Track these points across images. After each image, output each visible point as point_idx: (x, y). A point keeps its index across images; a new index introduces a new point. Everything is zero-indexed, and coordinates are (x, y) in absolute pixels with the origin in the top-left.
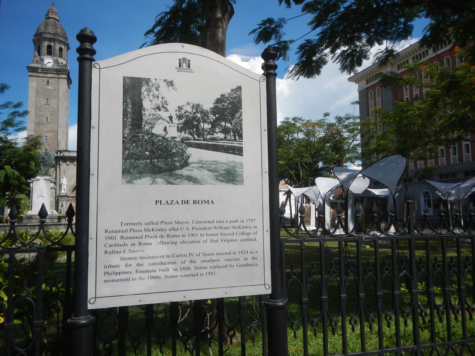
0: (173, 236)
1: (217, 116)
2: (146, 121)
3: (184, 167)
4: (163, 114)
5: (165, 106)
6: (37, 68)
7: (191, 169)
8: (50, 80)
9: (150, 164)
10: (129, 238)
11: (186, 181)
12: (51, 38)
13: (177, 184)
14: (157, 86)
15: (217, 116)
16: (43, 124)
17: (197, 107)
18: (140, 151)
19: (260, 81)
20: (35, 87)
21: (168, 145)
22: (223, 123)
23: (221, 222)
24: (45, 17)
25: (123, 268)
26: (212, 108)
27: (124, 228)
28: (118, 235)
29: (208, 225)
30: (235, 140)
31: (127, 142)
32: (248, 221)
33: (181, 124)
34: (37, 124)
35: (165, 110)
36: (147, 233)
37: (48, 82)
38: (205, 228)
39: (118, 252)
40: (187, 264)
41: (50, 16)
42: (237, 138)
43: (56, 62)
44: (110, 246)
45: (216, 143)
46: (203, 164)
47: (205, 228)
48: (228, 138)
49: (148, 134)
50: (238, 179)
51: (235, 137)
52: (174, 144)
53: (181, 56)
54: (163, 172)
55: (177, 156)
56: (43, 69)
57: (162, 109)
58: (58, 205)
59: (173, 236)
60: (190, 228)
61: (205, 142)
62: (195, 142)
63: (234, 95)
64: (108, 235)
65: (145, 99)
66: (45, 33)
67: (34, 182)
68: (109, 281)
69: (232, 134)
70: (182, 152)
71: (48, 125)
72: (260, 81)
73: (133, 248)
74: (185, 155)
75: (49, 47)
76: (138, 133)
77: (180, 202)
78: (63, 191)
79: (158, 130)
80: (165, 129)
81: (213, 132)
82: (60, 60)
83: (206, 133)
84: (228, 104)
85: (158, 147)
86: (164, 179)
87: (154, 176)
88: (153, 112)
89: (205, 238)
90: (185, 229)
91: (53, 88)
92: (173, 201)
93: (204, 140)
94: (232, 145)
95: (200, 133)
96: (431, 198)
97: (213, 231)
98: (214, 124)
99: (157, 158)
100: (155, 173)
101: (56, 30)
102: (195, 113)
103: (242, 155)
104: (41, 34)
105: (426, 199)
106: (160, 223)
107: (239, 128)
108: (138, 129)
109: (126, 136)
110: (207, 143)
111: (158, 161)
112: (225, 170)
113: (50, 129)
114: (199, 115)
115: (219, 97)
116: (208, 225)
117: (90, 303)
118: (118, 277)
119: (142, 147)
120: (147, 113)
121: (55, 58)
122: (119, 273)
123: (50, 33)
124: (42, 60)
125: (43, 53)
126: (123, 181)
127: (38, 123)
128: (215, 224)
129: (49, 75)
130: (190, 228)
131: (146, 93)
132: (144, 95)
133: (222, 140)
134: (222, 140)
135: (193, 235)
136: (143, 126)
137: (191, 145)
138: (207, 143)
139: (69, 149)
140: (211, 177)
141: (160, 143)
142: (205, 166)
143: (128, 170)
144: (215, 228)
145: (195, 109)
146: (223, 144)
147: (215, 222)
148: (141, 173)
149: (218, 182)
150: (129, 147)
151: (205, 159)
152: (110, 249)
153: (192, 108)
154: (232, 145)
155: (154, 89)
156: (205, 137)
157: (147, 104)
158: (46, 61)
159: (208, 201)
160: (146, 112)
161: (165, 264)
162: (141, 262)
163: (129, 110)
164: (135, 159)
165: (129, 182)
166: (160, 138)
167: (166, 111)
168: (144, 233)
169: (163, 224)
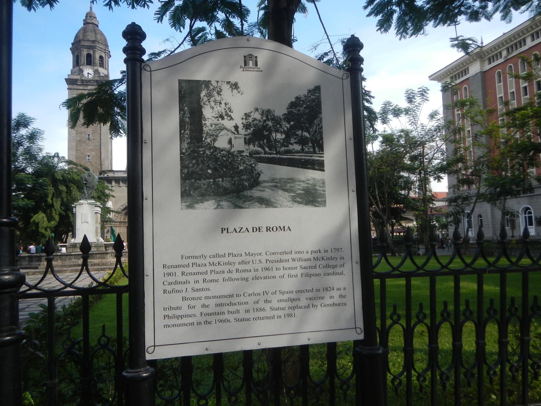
0: (243, 271)
1: (292, 123)
2: (207, 133)
3: (254, 187)
4: (227, 123)
5: (230, 113)
6: (76, 80)
7: (262, 189)
9: (213, 184)
10: (191, 274)
11: (256, 204)
12: (90, 46)
13: (246, 208)
14: (219, 90)
15: (292, 123)
16: (84, 142)
17: (267, 113)
18: (202, 170)
19: (342, 79)
21: (234, 160)
22: (299, 132)
23: (300, 252)
24: (82, 22)
25: (185, 311)
26: (285, 114)
27: (185, 262)
28: (179, 271)
29: (285, 257)
30: (314, 152)
31: (186, 158)
32: (333, 250)
33: (248, 135)
34: (78, 143)
35: (229, 118)
36: (213, 268)
38: (281, 261)
39: (179, 291)
40: (261, 305)
41: (88, 21)
42: (317, 149)
43: (96, 72)
44: (170, 284)
45: (291, 157)
46: (277, 182)
47: (281, 261)
48: (306, 150)
49: (210, 148)
50: (319, 200)
51: (314, 149)
52: (241, 159)
53: (246, 52)
54: (229, 193)
55: (244, 173)
56: (83, 81)
57: (226, 117)
59: (243, 271)
60: (264, 261)
61: (278, 156)
62: (267, 156)
63: (312, 97)
64: (167, 271)
65: (205, 106)
66: (84, 40)
67: (77, 207)
68: (169, 326)
69: (310, 145)
70: (252, 170)
71: (90, 143)
72: (342, 79)
73: (197, 286)
74: (255, 172)
75: (89, 56)
76: (198, 147)
77: (250, 230)
79: (222, 143)
80: (230, 142)
81: (287, 143)
82: (102, 71)
83: (279, 145)
84: (305, 108)
85: (222, 164)
86: (230, 201)
87: (219, 199)
88: (215, 121)
89: (281, 272)
90: (258, 262)
92: (242, 228)
93: (276, 154)
94: (310, 158)
95: (272, 145)
96: (533, 215)
97: (291, 264)
98: (289, 134)
99: (222, 177)
100: (219, 195)
101: (96, 37)
102: (265, 121)
103: (323, 171)
104: (80, 41)
105: (527, 215)
106: (227, 255)
107: (319, 138)
108: (198, 143)
109: (184, 151)
110: (281, 156)
111: (223, 181)
112: (304, 190)
113: (93, 147)
114: (270, 123)
115: (294, 100)
116: (285, 257)
117: (148, 352)
118: (180, 321)
119: (204, 164)
120: (208, 123)
121: (96, 68)
122: (181, 317)
123: (89, 40)
124: (81, 71)
125: (82, 63)
126: (182, 206)
127: (79, 141)
128: (294, 256)
130: (264, 261)
131: (205, 99)
132: (204, 101)
133: (298, 152)
134: (298, 152)
135: (267, 269)
136: (204, 139)
137: (261, 160)
138: (281, 156)
139: (114, 169)
140: (287, 199)
141: (225, 159)
142: (279, 185)
143: (187, 192)
144: (294, 260)
145: (265, 116)
146: (300, 157)
147: (293, 252)
148: (203, 195)
149: (296, 205)
150: (189, 164)
151: (278, 176)
152: (169, 288)
153: (262, 115)
154: (310, 158)
155: (215, 93)
156: (278, 149)
157: (208, 113)
158: (85, 73)
159: (284, 227)
160: (206, 122)
161: (235, 304)
162: (207, 302)
163: (187, 120)
164: (196, 179)
165: (190, 207)
166: (224, 152)
167: (230, 120)
168: (209, 268)
169: (231, 256)
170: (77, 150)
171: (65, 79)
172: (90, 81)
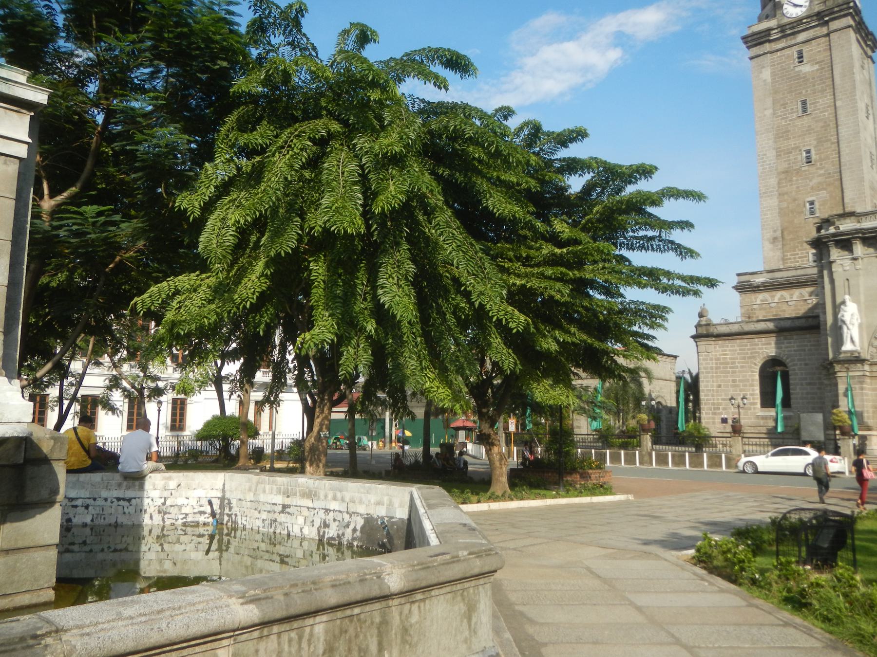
6: (769, 30)
8: (805, 49)
16: (798, 172)
20: (769, 80)
34: (783, 176)
37: (800, 57)
56: (782, 28)
58: (837, 390)
71: (812, 169)
78: (847, 346)
91: (816, 67)
113: (820, 179)
127: (786, 172)
129: (802, 37)
170: (781, 195)
171: (743, 38)
172: (799, 21)
